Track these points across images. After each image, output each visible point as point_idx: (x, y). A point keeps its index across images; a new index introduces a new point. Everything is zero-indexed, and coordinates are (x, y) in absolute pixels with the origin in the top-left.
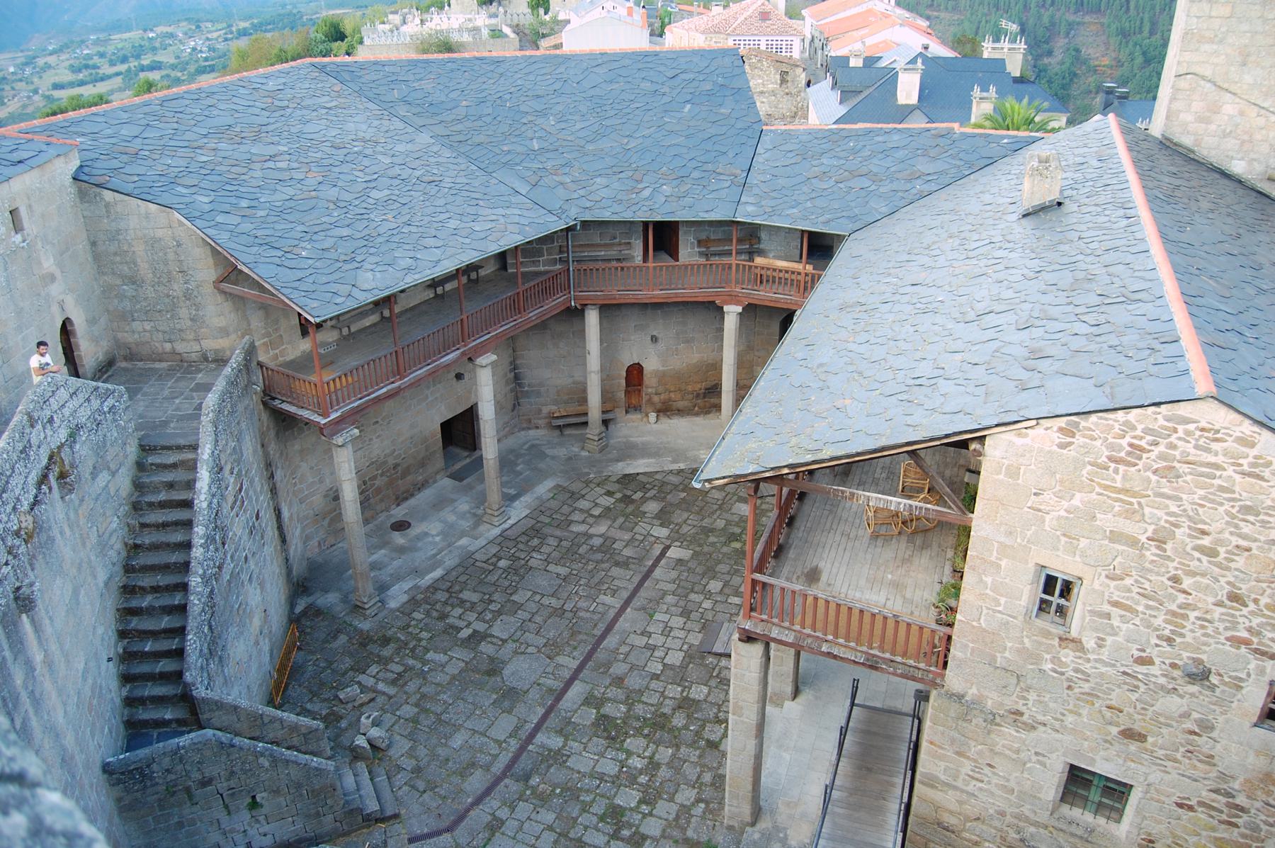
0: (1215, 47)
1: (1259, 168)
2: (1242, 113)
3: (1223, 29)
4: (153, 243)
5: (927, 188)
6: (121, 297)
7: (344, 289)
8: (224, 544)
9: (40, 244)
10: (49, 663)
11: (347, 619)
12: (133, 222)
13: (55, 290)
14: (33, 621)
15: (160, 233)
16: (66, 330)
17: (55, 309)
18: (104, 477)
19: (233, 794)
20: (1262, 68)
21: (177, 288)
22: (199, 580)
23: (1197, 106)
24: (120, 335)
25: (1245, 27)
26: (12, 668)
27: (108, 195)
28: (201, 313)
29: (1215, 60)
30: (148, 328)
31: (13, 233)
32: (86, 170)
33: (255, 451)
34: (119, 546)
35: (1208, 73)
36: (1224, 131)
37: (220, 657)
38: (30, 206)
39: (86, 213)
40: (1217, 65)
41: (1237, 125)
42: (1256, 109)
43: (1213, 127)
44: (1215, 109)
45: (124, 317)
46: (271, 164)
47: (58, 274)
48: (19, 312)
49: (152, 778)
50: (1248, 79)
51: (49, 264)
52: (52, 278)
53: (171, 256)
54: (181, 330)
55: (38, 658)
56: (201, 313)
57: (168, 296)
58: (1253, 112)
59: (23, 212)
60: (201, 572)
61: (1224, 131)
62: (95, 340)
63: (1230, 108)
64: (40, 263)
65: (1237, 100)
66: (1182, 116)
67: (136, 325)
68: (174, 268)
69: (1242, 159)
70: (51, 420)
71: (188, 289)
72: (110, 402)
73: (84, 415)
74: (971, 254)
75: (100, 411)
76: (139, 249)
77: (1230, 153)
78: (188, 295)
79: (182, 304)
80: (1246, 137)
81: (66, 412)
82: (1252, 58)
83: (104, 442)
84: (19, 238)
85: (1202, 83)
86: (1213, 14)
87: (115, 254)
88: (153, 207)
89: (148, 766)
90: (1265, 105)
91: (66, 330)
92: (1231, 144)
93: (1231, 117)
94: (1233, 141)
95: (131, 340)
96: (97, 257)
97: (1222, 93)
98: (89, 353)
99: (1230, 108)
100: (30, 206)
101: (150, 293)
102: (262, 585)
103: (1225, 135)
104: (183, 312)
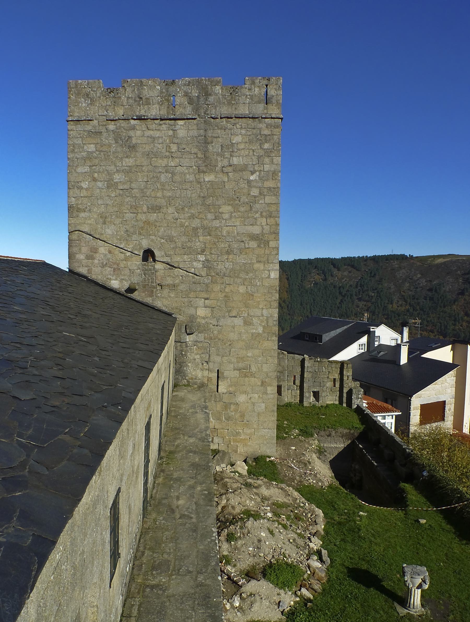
2: (110, 252)
20: (114, 224)
23: (85, 249)
25: (100, 202)
29: (89, 222)
36: (102, 263)
40: (91, 224)
41: (108, 259)
43: (96, 261)
44: (95, 250)
50: (109, 231)
58: (117, 251)
61: (102, 263)
63: (103, 250)
66: (77, 256)
69: (116, 279)
77: (109, 276)
80: (115, 266)
82: (109, 219)
86: (82, 195)
90: (122, 246)
93: (105, 255)
94: (109, 269)
99: (103, 250)
103: (103, 266)
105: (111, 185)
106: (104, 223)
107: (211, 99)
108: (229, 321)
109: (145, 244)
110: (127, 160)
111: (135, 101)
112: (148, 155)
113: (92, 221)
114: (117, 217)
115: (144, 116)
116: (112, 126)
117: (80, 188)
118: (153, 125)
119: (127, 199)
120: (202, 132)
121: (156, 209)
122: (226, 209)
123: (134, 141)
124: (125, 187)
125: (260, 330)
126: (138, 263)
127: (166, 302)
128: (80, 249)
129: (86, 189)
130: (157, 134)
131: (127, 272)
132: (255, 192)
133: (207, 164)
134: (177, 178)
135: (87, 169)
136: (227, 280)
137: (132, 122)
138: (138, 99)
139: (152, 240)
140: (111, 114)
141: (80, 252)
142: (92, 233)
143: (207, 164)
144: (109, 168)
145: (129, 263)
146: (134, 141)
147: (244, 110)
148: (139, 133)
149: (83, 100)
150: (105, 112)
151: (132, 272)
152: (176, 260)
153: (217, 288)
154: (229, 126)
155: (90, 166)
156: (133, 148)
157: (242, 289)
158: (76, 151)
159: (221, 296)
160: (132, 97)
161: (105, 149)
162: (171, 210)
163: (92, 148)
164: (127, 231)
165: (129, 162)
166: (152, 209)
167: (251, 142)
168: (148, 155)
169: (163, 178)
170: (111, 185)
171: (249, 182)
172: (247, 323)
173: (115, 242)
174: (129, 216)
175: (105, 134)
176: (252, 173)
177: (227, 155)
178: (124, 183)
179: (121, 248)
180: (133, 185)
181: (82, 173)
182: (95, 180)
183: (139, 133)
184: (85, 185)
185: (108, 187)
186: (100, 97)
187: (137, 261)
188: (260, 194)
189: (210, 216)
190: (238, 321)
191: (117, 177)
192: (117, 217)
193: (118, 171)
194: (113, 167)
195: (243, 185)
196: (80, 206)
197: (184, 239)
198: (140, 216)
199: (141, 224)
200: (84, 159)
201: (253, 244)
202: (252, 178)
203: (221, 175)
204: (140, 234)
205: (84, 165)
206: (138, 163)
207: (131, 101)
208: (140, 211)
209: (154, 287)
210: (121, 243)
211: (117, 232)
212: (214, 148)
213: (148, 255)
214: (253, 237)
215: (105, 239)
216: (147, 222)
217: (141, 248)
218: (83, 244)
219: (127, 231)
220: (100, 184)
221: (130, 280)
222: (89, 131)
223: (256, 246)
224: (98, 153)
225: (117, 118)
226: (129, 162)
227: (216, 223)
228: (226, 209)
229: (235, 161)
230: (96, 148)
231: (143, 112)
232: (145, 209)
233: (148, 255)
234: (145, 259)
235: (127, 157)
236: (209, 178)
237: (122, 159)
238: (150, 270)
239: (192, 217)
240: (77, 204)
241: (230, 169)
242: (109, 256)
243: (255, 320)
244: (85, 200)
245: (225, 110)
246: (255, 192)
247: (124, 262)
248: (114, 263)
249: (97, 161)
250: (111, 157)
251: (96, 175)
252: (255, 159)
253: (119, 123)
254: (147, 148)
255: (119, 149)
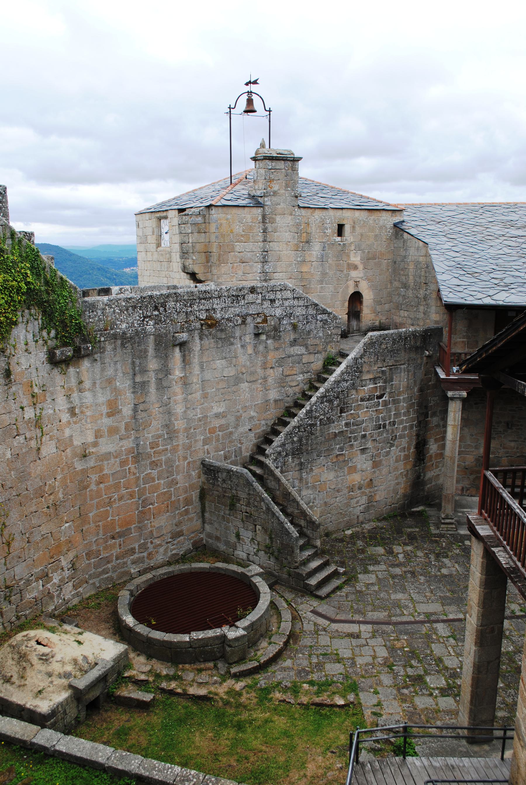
4: (417, 263)
6: (399, 295)
7: (480, 296)
8: (342, 412)
9: (353, 248)
10: (185, 382)
11: (431, 525)
12: (412, 252)
13: (354, 274)
14: (184, 357)
15: (421, 259)
16: (356, 298)
17: (351, 283)
18: (298, 350)
19: (247, 516)
21: (422, 293)
22: (305, 412)
24: (395, 317)
26: (149, 358)
27: (405, 234)
28: (429, 310)
30: (406, 315)
31: (336, 235)
32: (404, 224)
33: (408, 388)
34: (297, 389)
37: (301, 464)
38: (354, 227)
39: (395, 245)
45: (398, 307)
46: (513, 239)
47: (361, 267)
48: (324, 274)
49: (218, 481)
51: (356, 258)
52: (356, 268)
53: (423, 273)
54: (418, 319)
55: (178, 373)
56: (429, 310)
57: (417, 297)
59: (347, 229)
60: (308, 408)
62: (374, 311)
64: (348, 256)
67: (402, 313)
68: (423, 280)
70: (272, 301)
71: (426, 294)
72: (325, 317)
73: (299, 312)
75: (314, 317)
76: (411, 267)
78: (425, 298)
79: (422, 303)
81: (287, 303)
83: (309, 332)
84: (339, 239)
87: (402, 270)
88: (421, 243)
89: (218, 472)
91: (356, 298)
95: (398, 321)
96: (394, 270)
98: (368, 315)
100: (354, 227)
101: (410, 293)
102: (376, 465)
104: (422, 308)
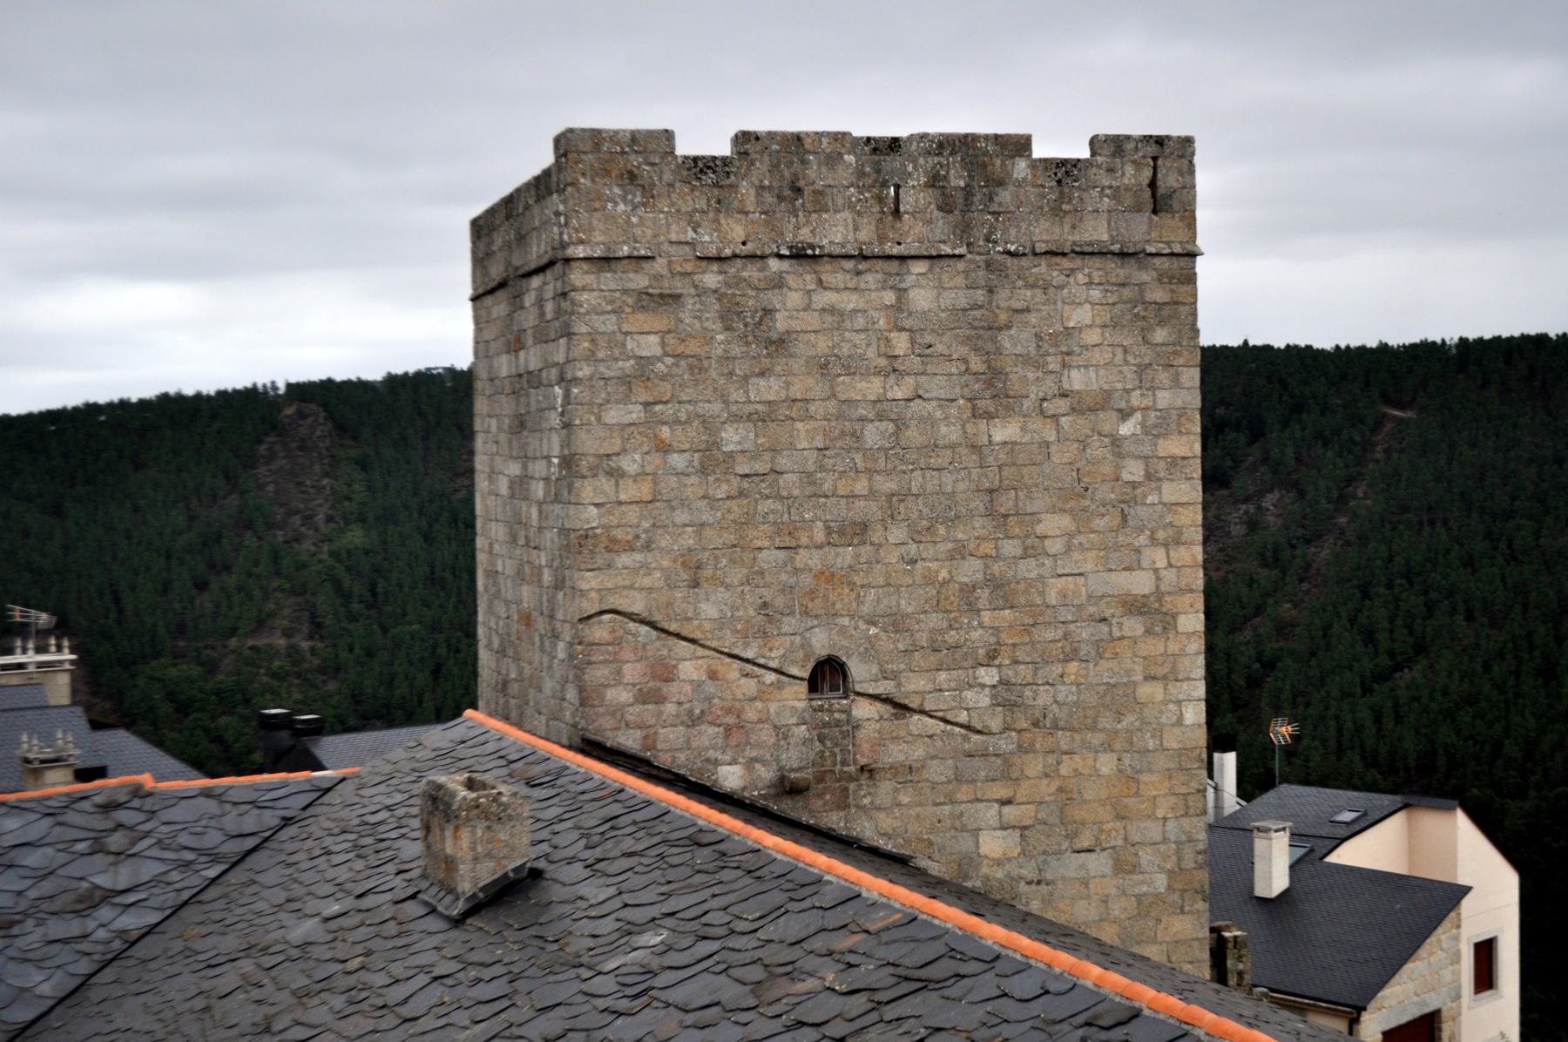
0: (639, 557)
1: (766, 774)
2: (713, 675)
3: (645, 524)
5: (132, 921)
20: (727, 587)
23: (632, 672)
25: (681, 517)
35: (638, 607)
36: (690, 712)
40: (650, 590)
41: (709, 699)
42: (737, 664)
43: (670, 708)
44: (665, 672)
50: (709, 610)
58: (732, 670)
61: (690, 712)
63: (690, 669)
65: (701, 651)
66: (610, 694)
69: (733, 762)
74: (406, 1011)
77: (711, 754)
80: (730, 720)
82: (708, 572)
85: (632, 626)
86: (623, 497)
90: (749, 654)
92: (708, 734)
93: (697, 685)
94: (712, 730)
97: (672, 641)
103: (693, 721)
105: (712, 460)
106: (695, 584)
107: (1005, 196)
108: (1071, 866)
109: (821, 643)
110: (762, 382)
111: (781, 198)
112: (823, 367)
113: (656, 579)
114: (733, 561)
115: (813, 247)
116: (711, 279)
117: (617, 475)
118: (836, 276)
119: (765, 506)
120: (980, 295)
121: (857, 532)
122: (1053, 524)
123: (781, 323)
124: (760, 467)
125: (1161, 882)
126: (801, 705)
127: (886, 822)
128: (619, 672)
129: (636, 478)
130: (850, 302)
131: (766, 735)
132: (1133, 471)
133: (993, 391)
134: (913, 435)
135: (635, 413)
136: (1063, 740)
137: (774, 264)
138: (787, 192)
139: (843, 631)
140: (708, 240)
141: (619, 683)
142: (657, 617)
143: (993, 391)
144: (703, 408)
145: (773, 707)
146: (781, 323)
147: (1097, 231)
148: (796, 302)
149: (617, 190)
150: (691, 234)
151: (782, 733)
152: (913, 686)
153: (1034, 765)
154: (1057, 277)
155: (646, 404)
156: (780, 344)
157: (1107, 764)
158: (601, 355)
159: (1047, 789)
160: (770, 188)
161: (693, 347)
162: (897, 533)
163: (650, 345)
164: (765, 605)
165: (768, 389)
166: (841, 533)
167: (1115, 324)
168: (823, 367)
169: (873, 435)
170: (712, 460)
171: (1116, 441)
172: (1125, 866)
173: (728, 641)
174: (770, 558)
175: (689, 303)
176: (1125, 415)
177: (1053, 363)
178: (755, 457)
179: (747, 661)
180: (783, 462)
181: (624, 427)
182: (664, 448)
183: (794, 298)
184: (629, 464)
185: (703, 471)
186: (671, 185)
187: (796, 696)
188: (1149, 476)
189: (1011, 548)
190: (1098, 864)
191: (732, 437)
192: (733, 561)
193: (735, 418)
194: (717, 407)
195: (1098, 449)
196: (619, 534)
197: (935, 620)
198: (803, 557)
199: (807, 580)
200: (626, 381)
201: (1133, 626)
202: (1126, 429)
203: (1036, 424)
204: (806, 613)
205: (626, 400)
206: (796, 391)
207: (769, 198)
208: (804, 541)
209: (851, 778)
210: (746, 645)
211: (735, 608)
212: (1016, 342)
213: (827, 674)
214: (1135, 606)
215: (697, 635)
216: (827, 576)
217: (807, 657)
218: (627, 654)
219: (765, 605)
220: (678, 461)
221: (778, 760)
222: (643, 293)
223: (1140, 630)
224: (669, 361)
225: (728, 252)
226: (768, 389)
227: (1028, 569)
228: (1053, 524)
229: (1076, 380)
230: (663, 344)
231: (805, 235)
232: (819, 535)
233: (827, 674)
234: (814, 684)
235: (762, 374)
236: (1004, 431)
237: (746, 378)
238: (838, 724)
239: (959, 553)
240: (607, 528)
241: (1062, 405)
242: (710, 688)
243: (1146, 857)
244: (632, 514)
245: (1044, 232)
246: (1133, 471)
247: (759, 705)
248: (729, 711)
249: (665, 389)
250: (714, 374)
251: (665, 432)
252: (1129, 372)
253: (732, 269)
254: (823, 344)
255: (736, 350)
